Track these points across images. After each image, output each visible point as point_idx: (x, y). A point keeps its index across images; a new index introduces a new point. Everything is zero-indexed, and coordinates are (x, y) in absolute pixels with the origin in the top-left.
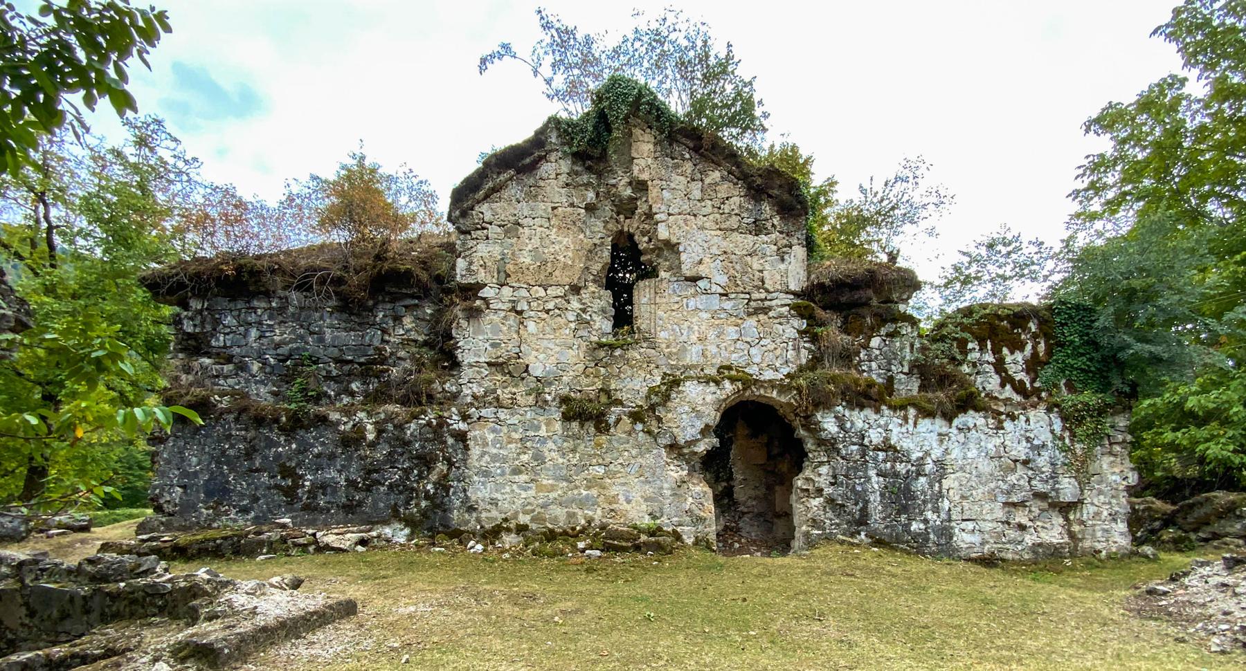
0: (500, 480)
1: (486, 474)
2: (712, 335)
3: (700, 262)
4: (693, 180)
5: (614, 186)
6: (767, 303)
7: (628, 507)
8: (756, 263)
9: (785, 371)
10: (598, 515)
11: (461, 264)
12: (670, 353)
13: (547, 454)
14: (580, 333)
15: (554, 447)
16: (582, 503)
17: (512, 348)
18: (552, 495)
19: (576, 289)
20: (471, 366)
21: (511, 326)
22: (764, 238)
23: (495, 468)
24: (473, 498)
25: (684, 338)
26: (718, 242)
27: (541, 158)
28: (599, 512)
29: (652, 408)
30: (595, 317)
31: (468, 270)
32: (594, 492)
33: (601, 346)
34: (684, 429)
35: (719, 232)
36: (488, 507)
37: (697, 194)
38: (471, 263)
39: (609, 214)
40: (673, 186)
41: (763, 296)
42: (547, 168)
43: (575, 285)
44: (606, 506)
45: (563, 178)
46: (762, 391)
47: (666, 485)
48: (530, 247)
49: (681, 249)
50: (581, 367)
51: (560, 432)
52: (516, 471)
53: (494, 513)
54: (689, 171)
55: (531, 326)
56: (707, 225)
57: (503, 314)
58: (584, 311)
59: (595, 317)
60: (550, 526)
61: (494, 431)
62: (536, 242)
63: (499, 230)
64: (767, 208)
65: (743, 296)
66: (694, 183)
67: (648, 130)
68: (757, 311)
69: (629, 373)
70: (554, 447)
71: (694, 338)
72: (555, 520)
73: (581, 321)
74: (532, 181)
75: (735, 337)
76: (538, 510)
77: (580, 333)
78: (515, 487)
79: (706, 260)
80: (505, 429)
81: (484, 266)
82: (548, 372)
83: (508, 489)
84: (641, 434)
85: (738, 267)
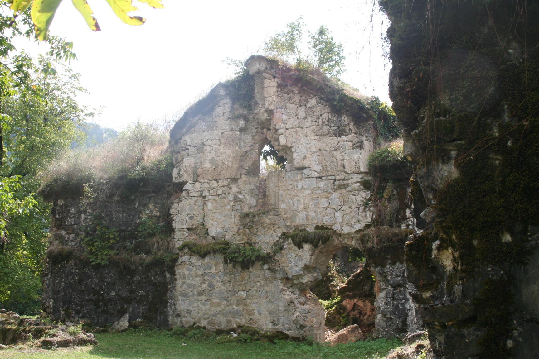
0: (192, 299)
1: (185, 295)
2: (312, 205)
3: (305, 158)
4: (300, 106)
5: (256, 114)
6: (345, 182)
7: (260, 317)
8: (338, 155)
9: (358, 227)
10: (243, 322)
11: (175, 171)
12: (286, 218)
13: (215, 284)
14: (235, 208)
15: (219, 280)
16: (235, 314)
17: (200, 219)
18: (219, 309)
19: (235, 180)
20: (179, 231)
21: (199, 206)
22: (344, 138)
23: (189, 292)
24: (179, 310)
25: (295, 207)
26: (315, 143)
27: (214, 105)
28: (243, 320)
29: (275, 253)
30: (247, 196)
31: (179, 174)
32: (241, 308)
33: (247, 215)
34: (292, 268)
35: (316, 137)
36: (186, 315)
37: (302, 114)
38: (180, 171)
39: (255, 131)
40: (288, 111)
41: (343, 177)
42: (219, 110)
43: (234, 178)
44: (247, 316)
45: (227, 115)
46: (346, 241)
47: (281, 304)
48: (210, 158)
49: (293, 150)
50: (236, 229)
51: (222, 270)
52: (200, 294)
53: (189, 319)
54: (297, 101)
55: (210, 205)
56: (309, 133)
57: (195, 199)
58: (240, 193)
59: (247, 196)
60: (217, 328)
61: (189, 270)
62: (213, 154)
63: (194, 149)
64: (345, 119)
65: (330, 178)
66: (300, 108)
67: (273, 79)
68: (340, 187)
69: (263, 232)
70: (219, 280)
71: (301, 207)
72: (220, 324)
73: (237, 200)
74: (211, 119)
75: (326, 205)
76: (211, 317)
77: (235, 208)
78: (199, 303)
79: (309, 156)
80: (194, 268)
81: (186, 171)
82: (218, 233)
83: (196, 305)
84: (267, 271)
85: (328, 159)
